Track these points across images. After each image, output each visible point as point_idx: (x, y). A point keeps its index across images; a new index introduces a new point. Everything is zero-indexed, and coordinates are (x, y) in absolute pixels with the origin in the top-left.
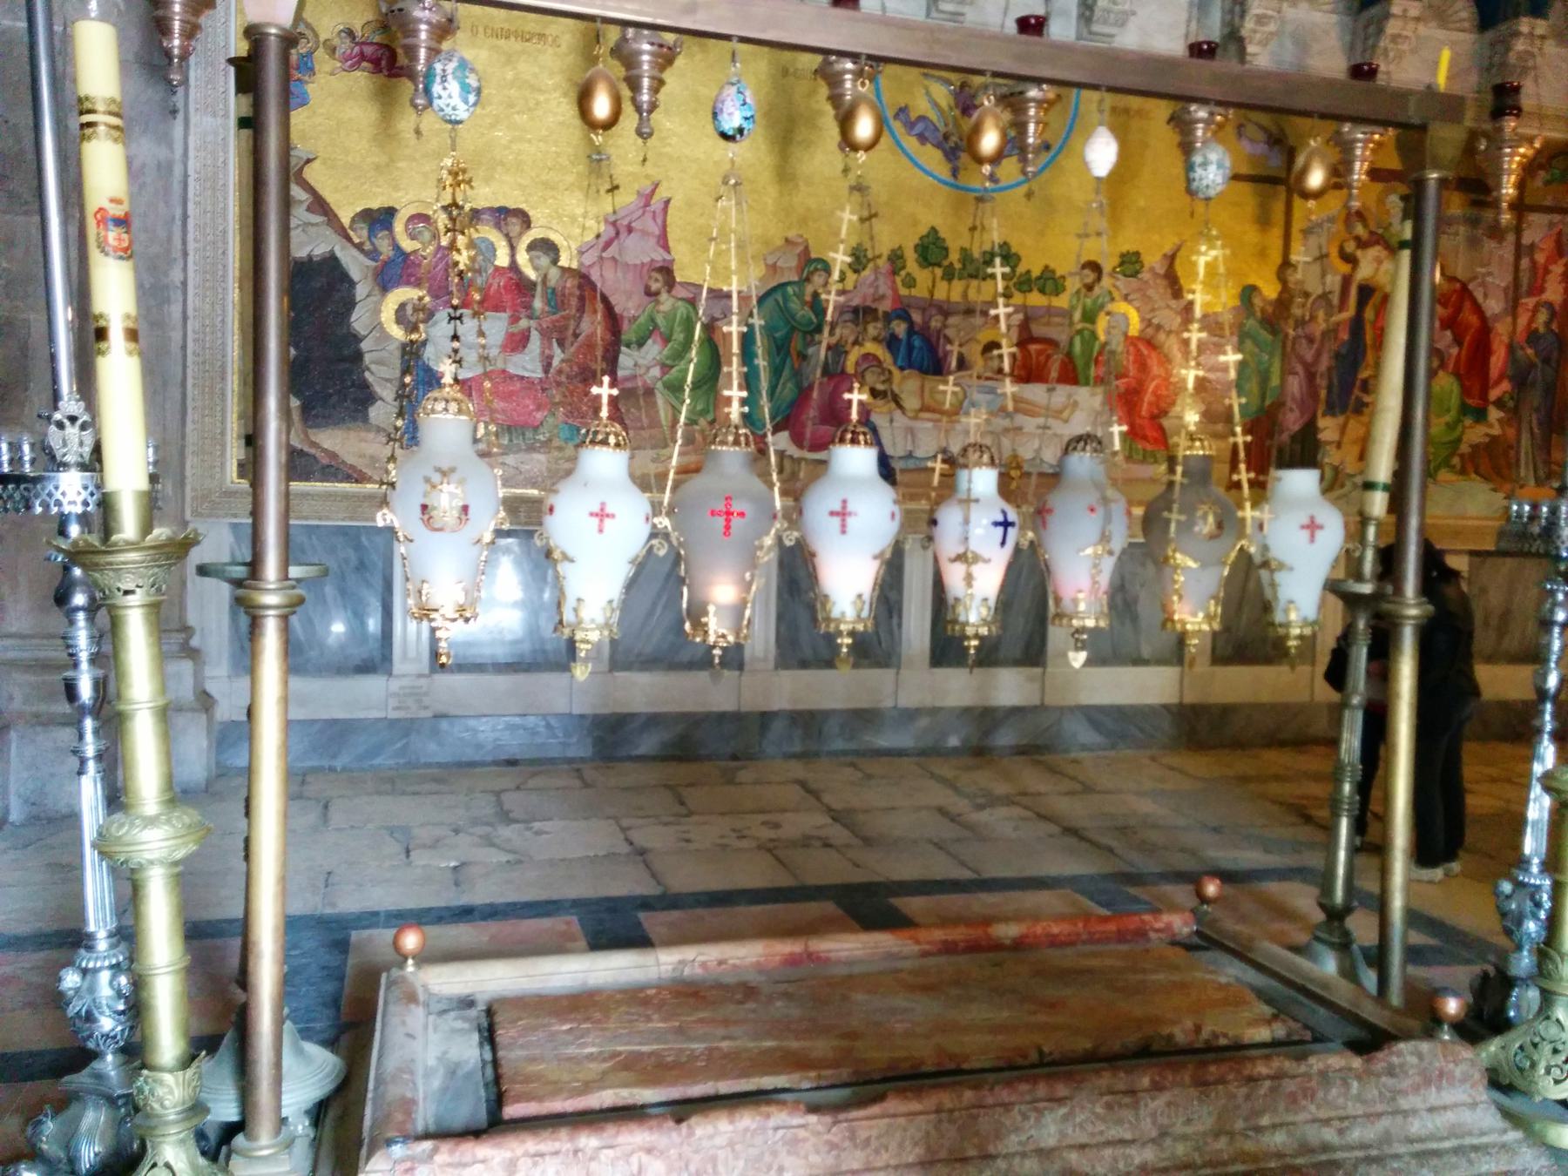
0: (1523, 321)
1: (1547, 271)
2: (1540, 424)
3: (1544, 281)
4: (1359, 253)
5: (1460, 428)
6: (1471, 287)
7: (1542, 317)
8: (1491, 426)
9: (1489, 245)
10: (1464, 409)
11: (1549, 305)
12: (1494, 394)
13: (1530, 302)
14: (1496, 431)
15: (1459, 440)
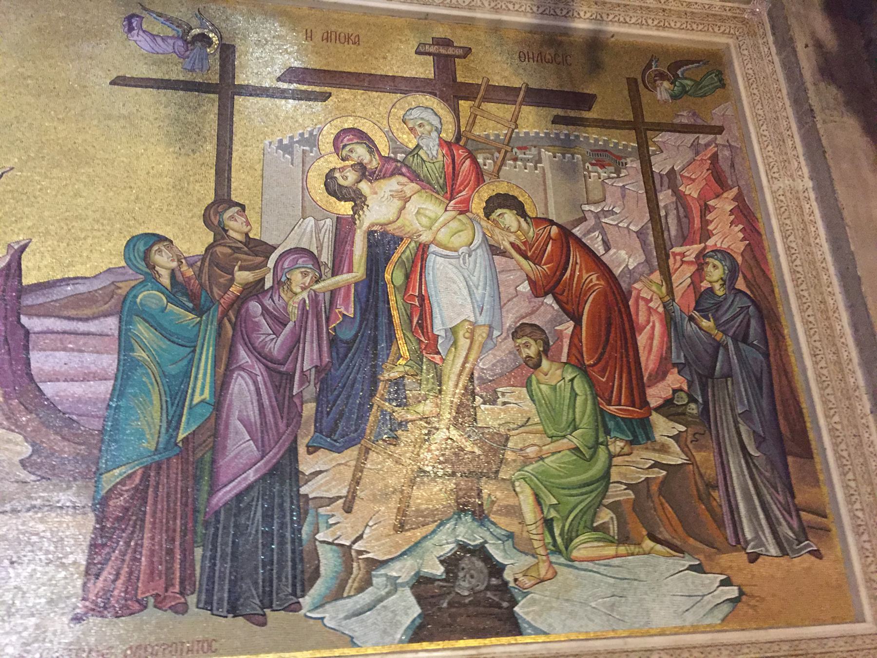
0: (682, 278)
1: (706, 209)
2: (759, 441)
3: (705, 223)
4: (364, 186)
5: (602, 453)
6: (577, 231)
7: (715, 273)
8: (664, 449)
9: (597, 175)
10: (602, 420)
11: (724, 254)
12: (656, 395)
13: (692, 251)
14: (676, 458)
15: (606, 476)
